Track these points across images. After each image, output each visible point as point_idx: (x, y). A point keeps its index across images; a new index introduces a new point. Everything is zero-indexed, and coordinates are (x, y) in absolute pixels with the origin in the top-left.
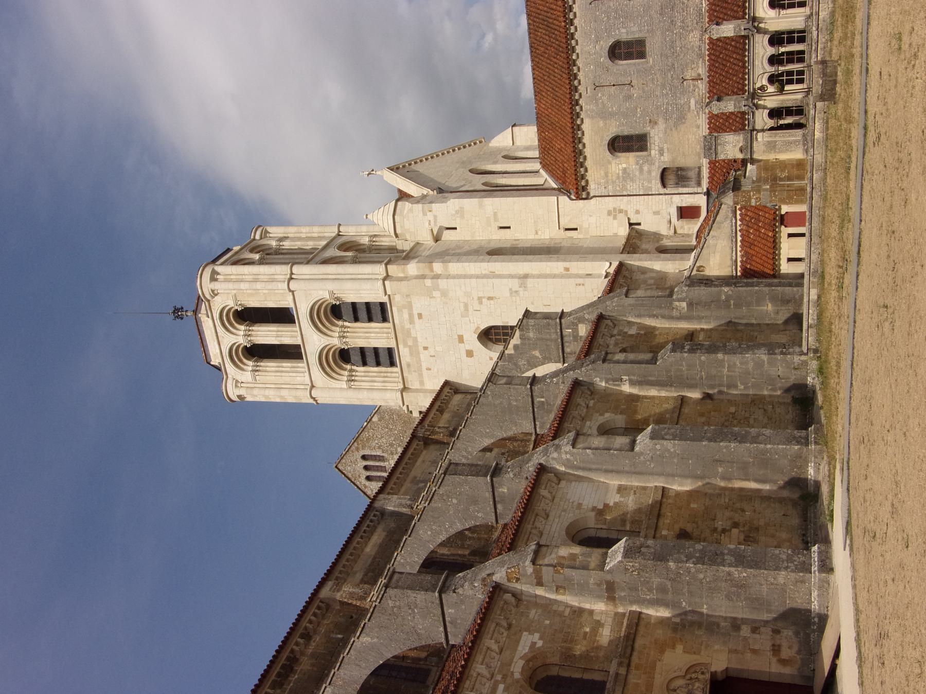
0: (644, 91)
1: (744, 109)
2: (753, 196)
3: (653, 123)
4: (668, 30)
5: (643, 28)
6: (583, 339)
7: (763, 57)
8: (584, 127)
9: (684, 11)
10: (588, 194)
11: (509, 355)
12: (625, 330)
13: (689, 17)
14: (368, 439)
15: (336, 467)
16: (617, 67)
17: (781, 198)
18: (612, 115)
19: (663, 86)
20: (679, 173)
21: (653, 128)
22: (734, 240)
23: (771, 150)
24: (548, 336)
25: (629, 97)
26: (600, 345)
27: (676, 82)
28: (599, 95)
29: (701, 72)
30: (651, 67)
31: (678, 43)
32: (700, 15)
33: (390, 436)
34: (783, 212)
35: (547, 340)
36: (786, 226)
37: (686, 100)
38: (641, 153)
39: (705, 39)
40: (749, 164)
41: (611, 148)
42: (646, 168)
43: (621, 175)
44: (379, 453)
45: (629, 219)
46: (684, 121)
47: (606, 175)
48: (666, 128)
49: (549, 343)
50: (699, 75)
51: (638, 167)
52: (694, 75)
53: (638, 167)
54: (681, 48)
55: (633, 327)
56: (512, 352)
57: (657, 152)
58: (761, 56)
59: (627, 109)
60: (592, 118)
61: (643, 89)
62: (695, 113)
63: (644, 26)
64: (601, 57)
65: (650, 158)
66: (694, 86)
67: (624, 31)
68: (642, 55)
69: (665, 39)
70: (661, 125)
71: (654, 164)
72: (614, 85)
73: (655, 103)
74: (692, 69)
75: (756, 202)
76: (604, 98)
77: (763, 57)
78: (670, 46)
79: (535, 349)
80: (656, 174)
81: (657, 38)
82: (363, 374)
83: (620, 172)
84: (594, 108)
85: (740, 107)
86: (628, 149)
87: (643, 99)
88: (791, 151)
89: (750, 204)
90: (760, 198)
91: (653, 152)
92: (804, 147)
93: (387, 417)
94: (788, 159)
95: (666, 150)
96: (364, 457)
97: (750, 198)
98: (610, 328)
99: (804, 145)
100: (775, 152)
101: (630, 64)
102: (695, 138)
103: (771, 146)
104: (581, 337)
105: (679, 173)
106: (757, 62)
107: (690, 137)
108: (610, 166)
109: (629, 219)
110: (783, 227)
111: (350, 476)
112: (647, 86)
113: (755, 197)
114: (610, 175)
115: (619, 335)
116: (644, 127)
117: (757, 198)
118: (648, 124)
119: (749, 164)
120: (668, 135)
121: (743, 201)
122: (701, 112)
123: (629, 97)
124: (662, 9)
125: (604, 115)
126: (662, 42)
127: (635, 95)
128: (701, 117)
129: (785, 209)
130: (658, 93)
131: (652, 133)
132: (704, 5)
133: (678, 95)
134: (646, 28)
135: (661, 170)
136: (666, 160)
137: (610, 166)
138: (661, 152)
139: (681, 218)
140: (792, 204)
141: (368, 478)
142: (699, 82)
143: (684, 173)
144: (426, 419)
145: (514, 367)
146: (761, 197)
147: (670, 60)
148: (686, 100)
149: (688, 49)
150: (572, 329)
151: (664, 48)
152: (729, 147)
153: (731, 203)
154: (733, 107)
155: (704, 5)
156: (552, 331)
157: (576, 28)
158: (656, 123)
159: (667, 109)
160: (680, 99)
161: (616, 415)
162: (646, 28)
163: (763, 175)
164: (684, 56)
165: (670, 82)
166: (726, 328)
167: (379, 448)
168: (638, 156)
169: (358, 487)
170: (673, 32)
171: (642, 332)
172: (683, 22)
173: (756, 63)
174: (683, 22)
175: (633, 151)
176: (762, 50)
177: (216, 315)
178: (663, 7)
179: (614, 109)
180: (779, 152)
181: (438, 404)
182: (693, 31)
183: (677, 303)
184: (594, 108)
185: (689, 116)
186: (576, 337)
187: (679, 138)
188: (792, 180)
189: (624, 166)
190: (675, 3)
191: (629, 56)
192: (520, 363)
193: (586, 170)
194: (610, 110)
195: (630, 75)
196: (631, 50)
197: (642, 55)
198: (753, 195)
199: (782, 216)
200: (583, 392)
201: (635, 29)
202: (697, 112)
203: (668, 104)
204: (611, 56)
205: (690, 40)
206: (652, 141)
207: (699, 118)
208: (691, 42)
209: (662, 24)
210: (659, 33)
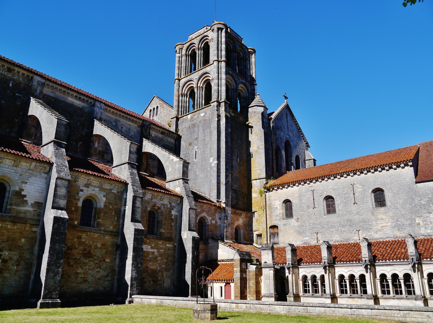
0: (311, 214)
1: (287, 263)
2: (238, 269)
3: (298, 219)
4: (340, 224)
5: (341, 212)
6: (174, 190)
7: (315, 272)
8: (295, 187)
9: (349, 231)
10: (267, 192)
11: (170, 157)
12: (175, 209)
13: (346, 234)
14: (163, 107)
15: (154, 97)
16: (322, 201)
17: (237, 283)
18: (300, 200)
19: (314, 224)
20: (276, 234)
21: (295, 220)
22: (221, 261)
23: (265, 277)
24: (176, 174)
25: (308, 207)
26: (161, 197)
27: (316, 230)
28: (309, 193)
29: (320, 242)
30: (322, 217)
31: (334, 229)
32: (347, 239)
33: (164, 116)
34: (231, 284)
35: (175, 174)
36: (225, 286)
37: (308, 235)
38: (284, 215)
39: (336, 243)
40: (256, 266)
41: (287, 201)
42: (278, 218)
43: (275, 206)
44: (159, 113)
45: (256, 212)
46: (299, 234)
47: (275, 200)
48: (295, 226)
49: (174, 174)
50: (319, 241)
51: (278, 214)
52: (319, 238)
53: (278, 214)
54: (332, 231)
55: (177, 213)
56: (171, 159)
57: (284, 223)
58: (316, 271)
59: (303, 207)
60: (299, 191)
61: (312, 214)
62: (302, 240)
63: (341, 212)
64: (327, 192)
65: (282, 219)
66: (314, 239)
67: (339, 202)
68: (329, 212)
69: (336, 223)
70: (296, 224)
71: (279, 221)
72: (314, 200)
73: (306, 220)
74: (322, 237)
75: (235, 271)
76: (308, 196)
77: (315, 272)
78: (333, 226)
79: (172, 168)
80: (275, 223)
81: (336, 219)
82: (185, 100)
83: (276, 206)
84: (303, 191)
85: (289, 261)
86: (287, 209)
87: (308, 214)
88: (265, 287)
89: (235, 267)
90: (237, 272)
91: (284, 221)
92: (267, 294)
93: (170, 114)
94: (261, 286)
95: (285, 227)
96: (157, 107)
97: (237, 267)
98: (176, 202)
99: (267, 294)
100: (264, 279)
101: (324, 207)
102: (291, 240)
103: (268, 278)
104: (175, 189)
105: (276, 234)
106: (313, 269)
107: (292, 238)
108: (278, 201)
109: (256, 212)
110: (225, 284)
111: (152, 103)
112: (314, 216)
113: (238, 270)
114: (275, 201)
115: (171, 206)
116: (296, 215)
117: (237, 271)
118: (297, 217)
119: (256, 266)
120: (292, 228)
121: (236, 264)
122: (303, 243)
123: (308, 207)
124: (350, 220)
125: (301, 196)
126: (334, 221)
127: (310, 210)
128: (300, 243)
129: (232, 285)
130: (311, 221)
131: (292, 220)
132: (352, 241)
133: (310, 231)
134: (341, 213)
135: (277, 225)
136: (281, 227)
137: (278, 201)
138: (285, 225)
139: (257, 236)
140: (234, 289)
141: (151, 110)
142: (316, 241)
143: (276, 236)
144: (156, 126)
145: (166, 160)
146: (238, 273)
147: (326, 226)
148: (308, 235)
149: (331, 235)
150: (178, 185)
151: (331, 223)
152: (267, 256)
153: (235, 258)
154: (289, 257)
155: (352, 241)
156: (178, 175)
157: (340, 178)
158: (297, 221)
159: (303, 226)
160: (308, 232)
161: (104, 203)
162: (341, 213)
163: (251, 273)
164: (328, 233)
165: (316, 227)
166: (176, 257)
167: (160, 112)
168: (283, 214)
169: (148, 107)
170: (339, 226)
171: (173, 217)
172: (344, 231)
173: (313, 269)
174: (344, 231)
175: (286, 211)
176: (318, 271)
177: (205, 34)
178: (351, 221)
179: (303, 201)
180: (264, 282)
181: (167, 132)
182: (340, 236)
183: (186, 233)
184: (303, 191)
185: (301, 237)
186: (175, 187)
187: (291, 233)
188: (249, 289)
189: (279, 208)
190: (353, 227)
191: (328, 206)
192: (167, 162)
193: (277, 190)
194: (303, 199)
195: (319, 207)
196: (331, 207)
197: (329, 212)
198: (238, 269)
199: (229, 284)
200: (121, 187)
201: (340, 207)
202: (303, 241)
203: (306, 226)
204: (328, 197)
205: (335, 235)
206: (289, 220)
207: (300, 242)
208: (335, 236)
209: (343, 221)
210: (339, 220)
